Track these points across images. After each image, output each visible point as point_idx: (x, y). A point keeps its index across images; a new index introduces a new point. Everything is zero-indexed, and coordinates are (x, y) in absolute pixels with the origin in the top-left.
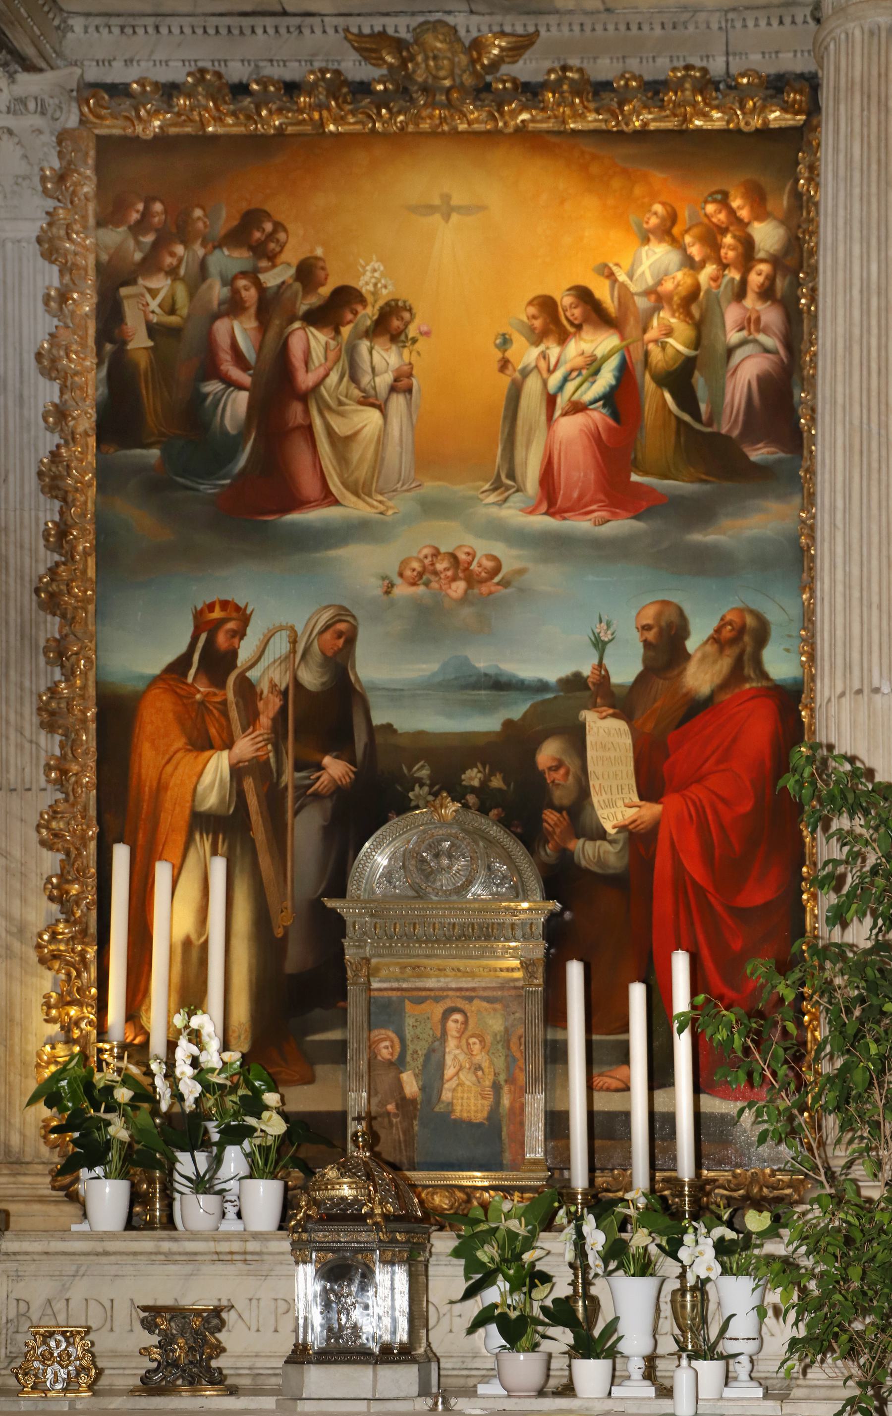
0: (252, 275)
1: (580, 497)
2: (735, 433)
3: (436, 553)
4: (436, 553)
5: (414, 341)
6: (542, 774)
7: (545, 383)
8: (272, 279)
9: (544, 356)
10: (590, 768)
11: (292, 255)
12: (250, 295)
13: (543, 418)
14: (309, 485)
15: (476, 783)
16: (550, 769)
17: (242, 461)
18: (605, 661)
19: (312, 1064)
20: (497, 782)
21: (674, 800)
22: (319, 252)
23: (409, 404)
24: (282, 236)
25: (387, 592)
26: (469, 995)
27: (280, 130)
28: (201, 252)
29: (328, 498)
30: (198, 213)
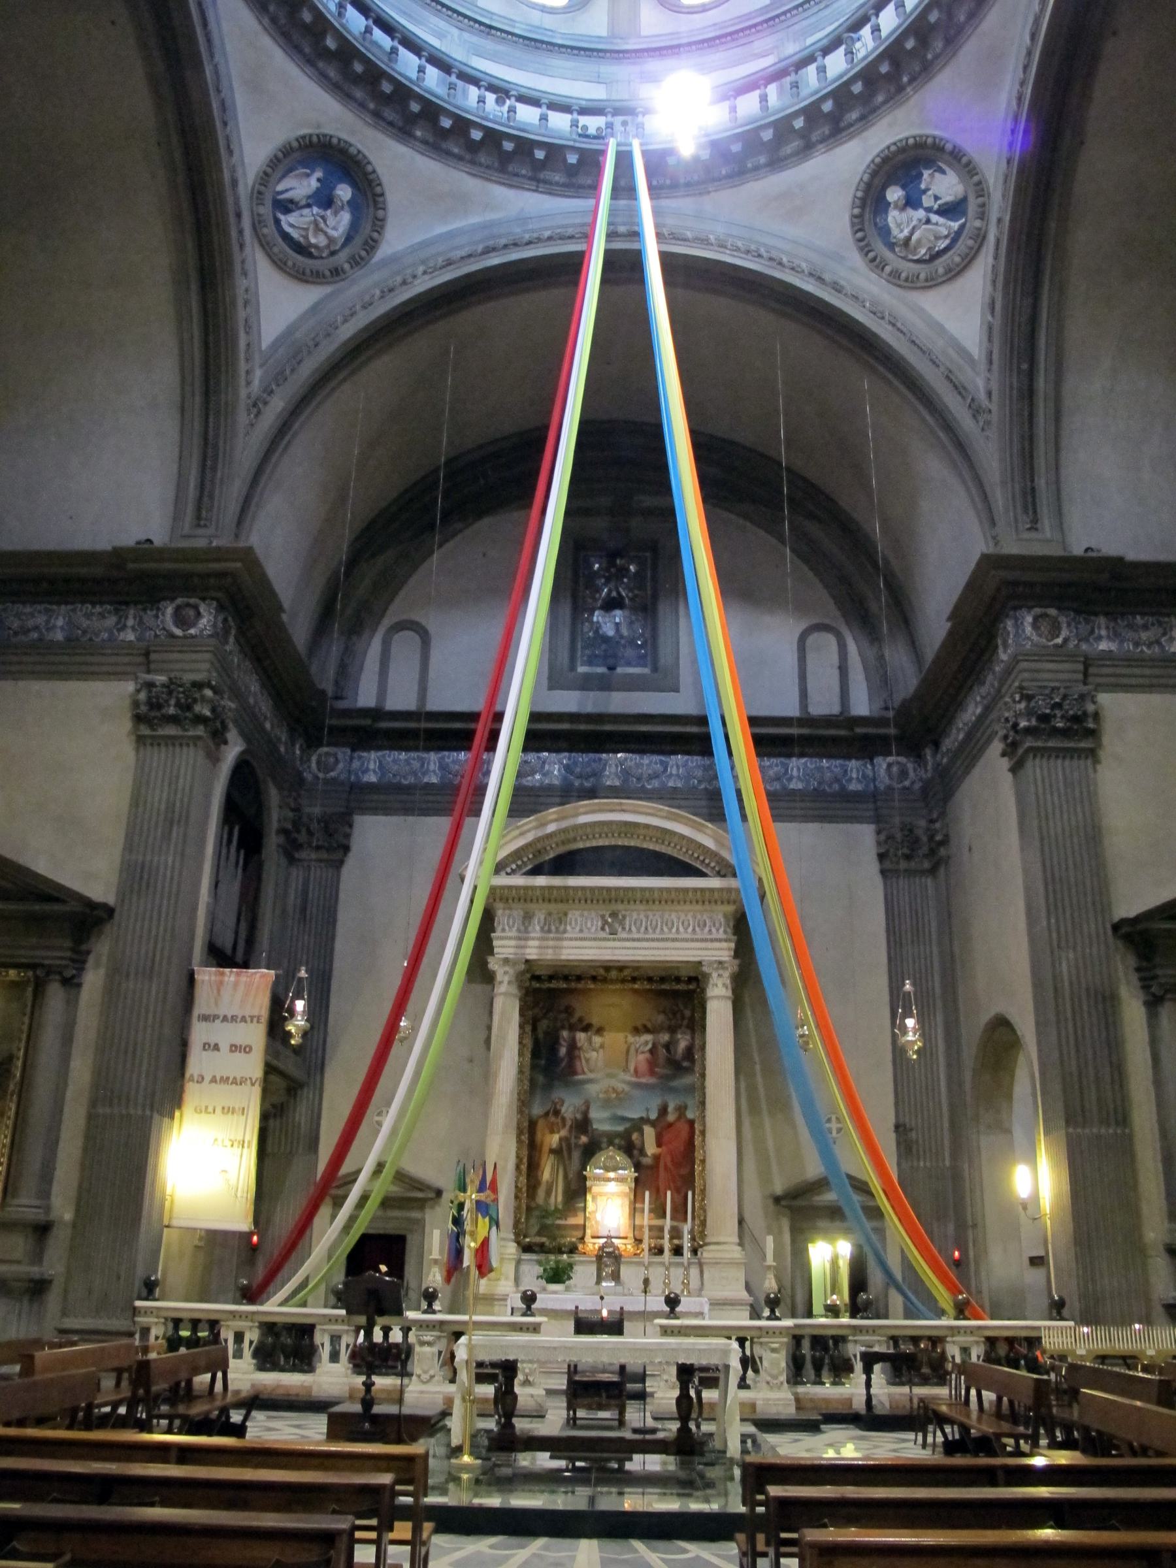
12: (566, 1024)
14: (579, 1069)
20: (623, 1143)
29: (584, 1073)
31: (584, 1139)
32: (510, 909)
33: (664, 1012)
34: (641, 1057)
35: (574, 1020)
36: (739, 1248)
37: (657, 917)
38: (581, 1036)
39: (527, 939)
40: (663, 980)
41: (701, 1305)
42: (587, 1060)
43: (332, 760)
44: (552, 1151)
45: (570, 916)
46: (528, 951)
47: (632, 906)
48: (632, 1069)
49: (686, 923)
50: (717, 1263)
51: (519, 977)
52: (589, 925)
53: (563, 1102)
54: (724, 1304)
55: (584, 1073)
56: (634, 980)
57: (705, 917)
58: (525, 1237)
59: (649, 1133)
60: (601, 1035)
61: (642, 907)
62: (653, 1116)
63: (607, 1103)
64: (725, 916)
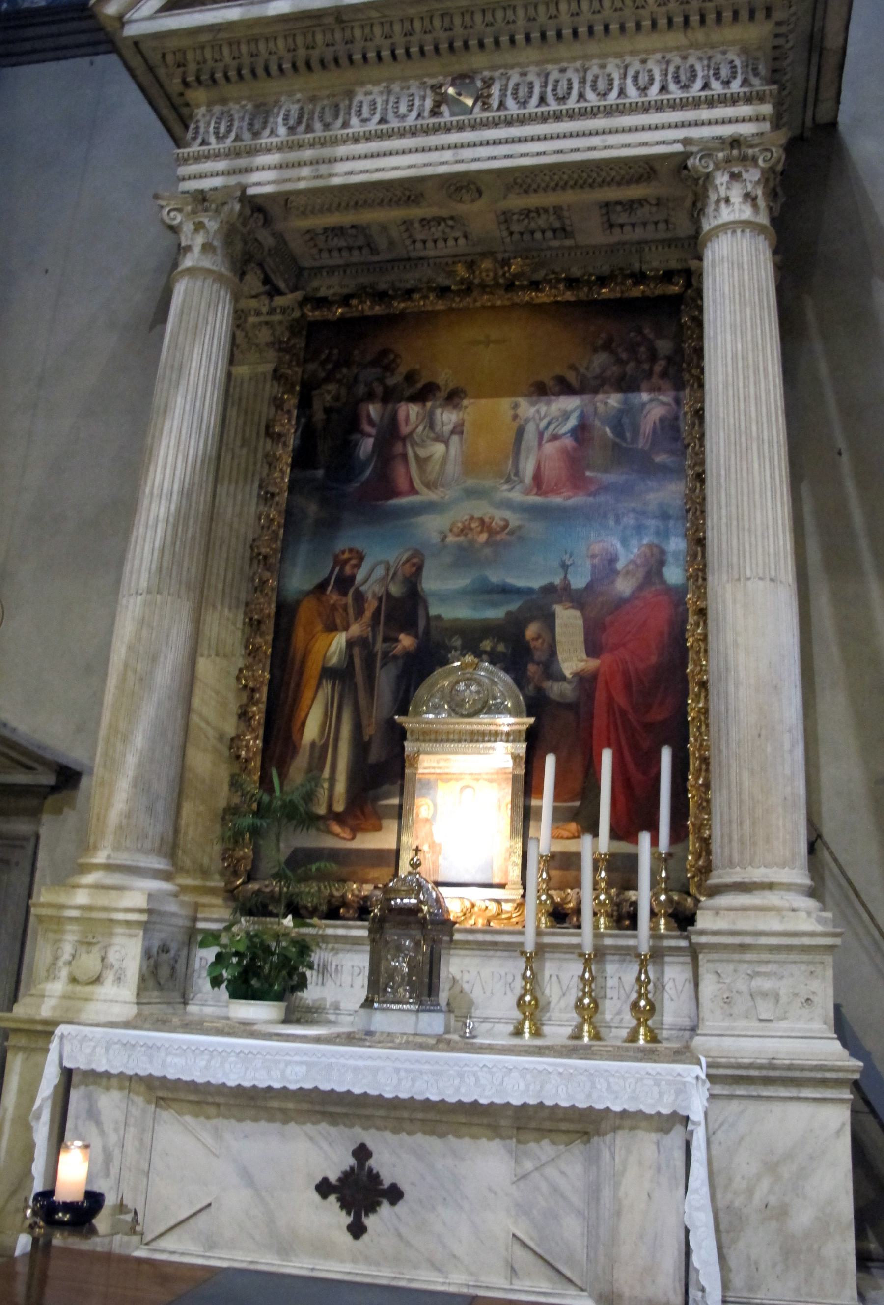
0: (381, 380)
1: (556, 485)
2: (647, 448)
3: (472, 518)
4: (472, 518)
5: (466, 407)
6: (528, 642)
7: (538, 426)
8: (391, 381)
9: (538, 411)
10: (558, 638)
11: (403, 370)
12: (379, 390)
13: (536, 443)
14: (402, 483)
15: (488, 648)
16: (533, 639)
17: (368, 473)
18: (569, 577)
19: (379, 818)
20: (501, 648)
21: (607, 657)
22: (417, 367)
23: (461, 440)
24: (399, 360)
25: (443, 540)
26: (476, 777)
27: (402, 312)
28: (355, 371)
29: (413, 491)
30: (356, 352)
31: (406, 641)
32: (224, 101)
33: (607, 346)
34: (550, 448)
36: (811, 904)
37: (570, 74)
38: (410, 412)
39: (252, 152)
41: (681, 1089)
42: (422, 462)
44: (327, 673)
45: (359, 97)
46: (255, 177)
47: (507, 57)
48: (528, 468)
49: (643, 79)
50: (743, 948)
51: (230, 234)
52: (403, 109)
53: (361, 558)
54: (767, 1081)
55: (413, 491)
57: (692, 60)
58: (250, 878)
60: (456, 407)
61: (531, 54)
64: (744, 51)
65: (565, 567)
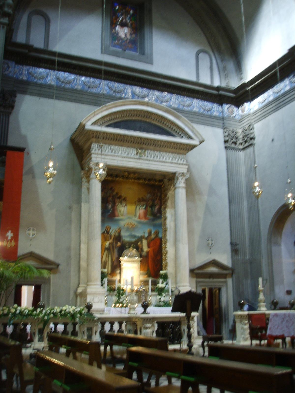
31: (119, 244)
35: (114, 193)
38: (117, 201)
40: (150, 180)
42: (120, 211)
43: (6, 66)
48: (138, 214)
56: (139, 179)
59: (145, 243)
62: (146, 235)
63: (128, 229)
65: (144, 233)
